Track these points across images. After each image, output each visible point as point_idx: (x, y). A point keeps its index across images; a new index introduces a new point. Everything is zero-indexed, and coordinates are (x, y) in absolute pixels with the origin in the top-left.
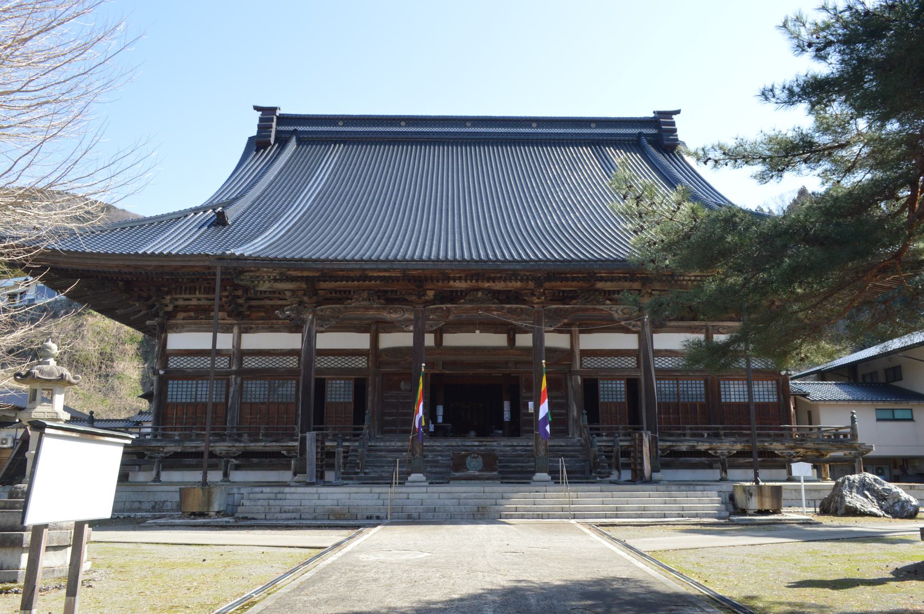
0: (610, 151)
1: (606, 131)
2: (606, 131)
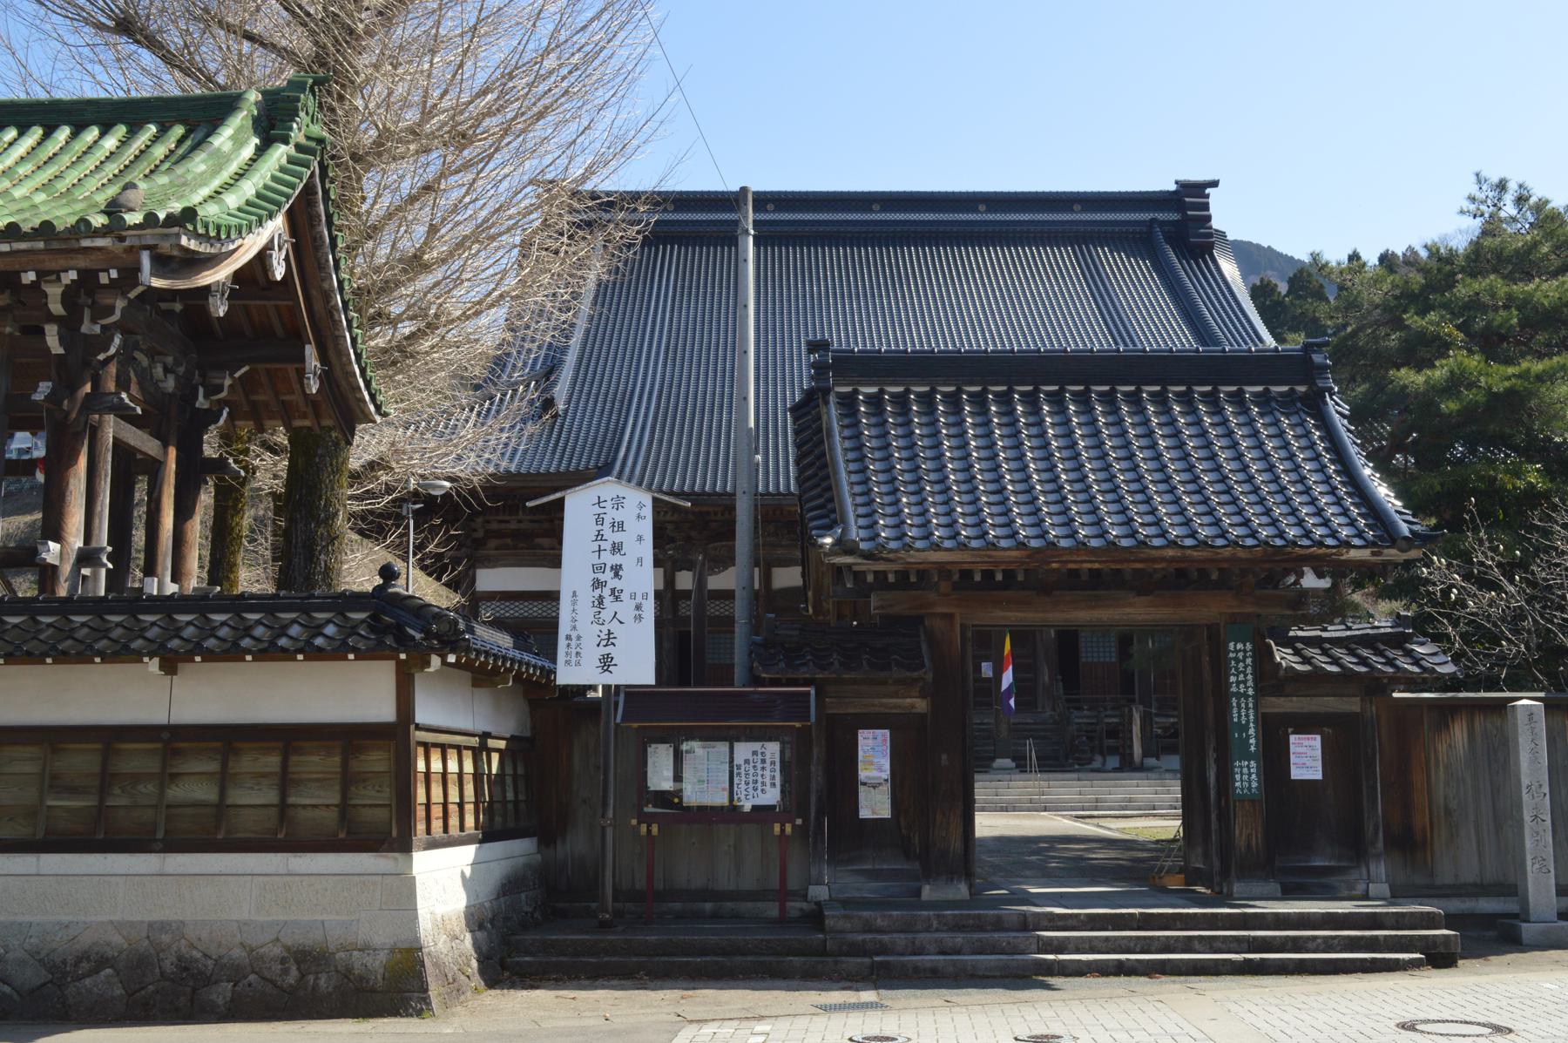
0: (1103, 254)
1: (1098, 217)
2: (1098, 217)
